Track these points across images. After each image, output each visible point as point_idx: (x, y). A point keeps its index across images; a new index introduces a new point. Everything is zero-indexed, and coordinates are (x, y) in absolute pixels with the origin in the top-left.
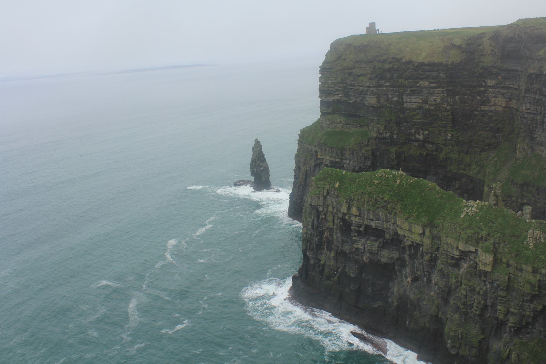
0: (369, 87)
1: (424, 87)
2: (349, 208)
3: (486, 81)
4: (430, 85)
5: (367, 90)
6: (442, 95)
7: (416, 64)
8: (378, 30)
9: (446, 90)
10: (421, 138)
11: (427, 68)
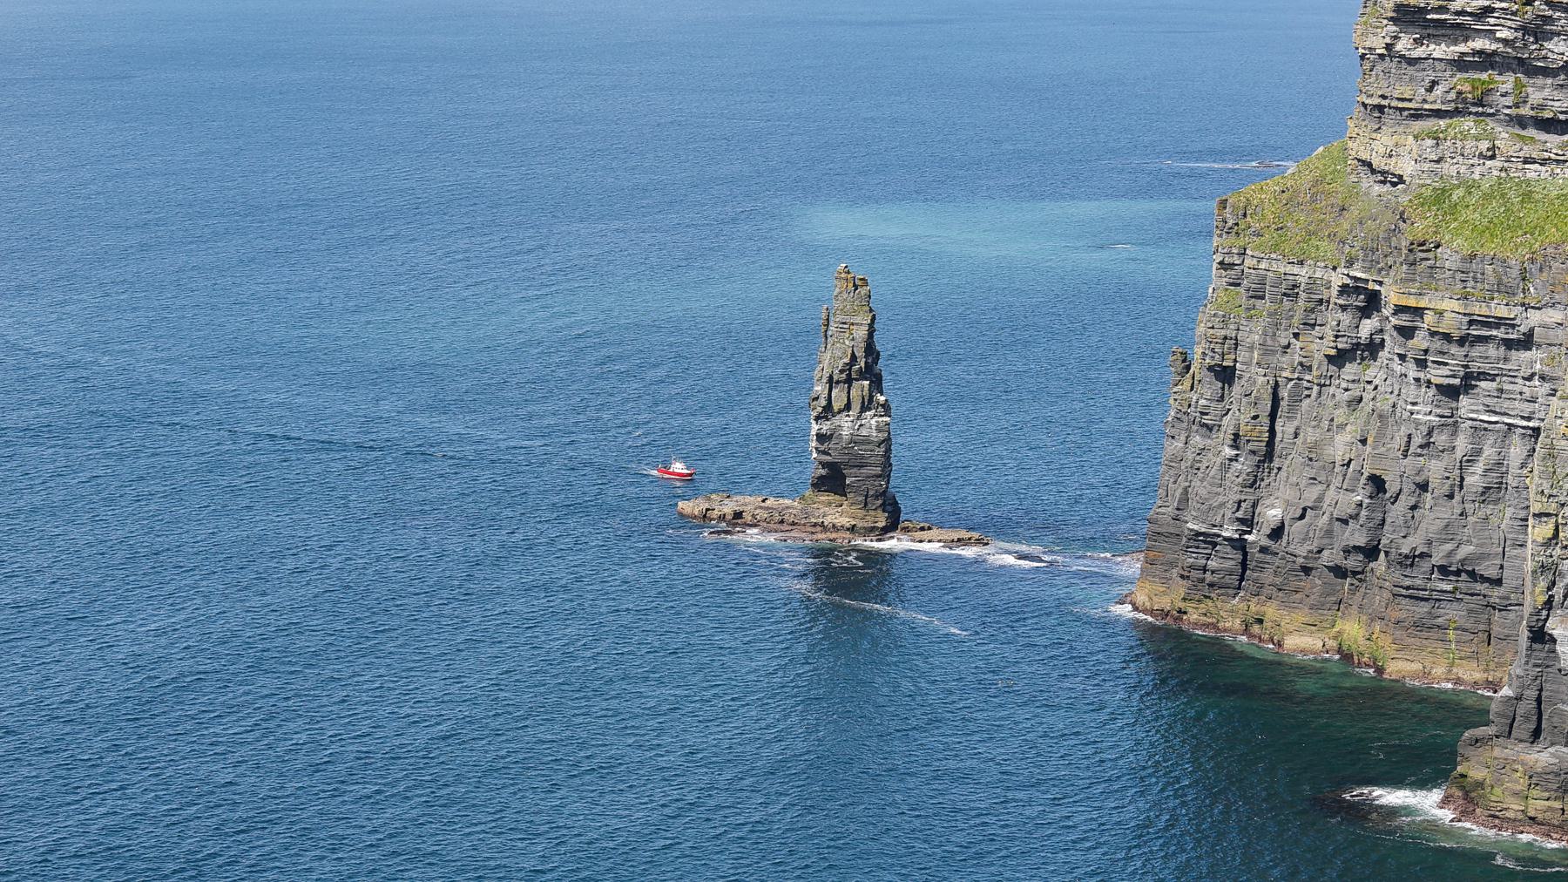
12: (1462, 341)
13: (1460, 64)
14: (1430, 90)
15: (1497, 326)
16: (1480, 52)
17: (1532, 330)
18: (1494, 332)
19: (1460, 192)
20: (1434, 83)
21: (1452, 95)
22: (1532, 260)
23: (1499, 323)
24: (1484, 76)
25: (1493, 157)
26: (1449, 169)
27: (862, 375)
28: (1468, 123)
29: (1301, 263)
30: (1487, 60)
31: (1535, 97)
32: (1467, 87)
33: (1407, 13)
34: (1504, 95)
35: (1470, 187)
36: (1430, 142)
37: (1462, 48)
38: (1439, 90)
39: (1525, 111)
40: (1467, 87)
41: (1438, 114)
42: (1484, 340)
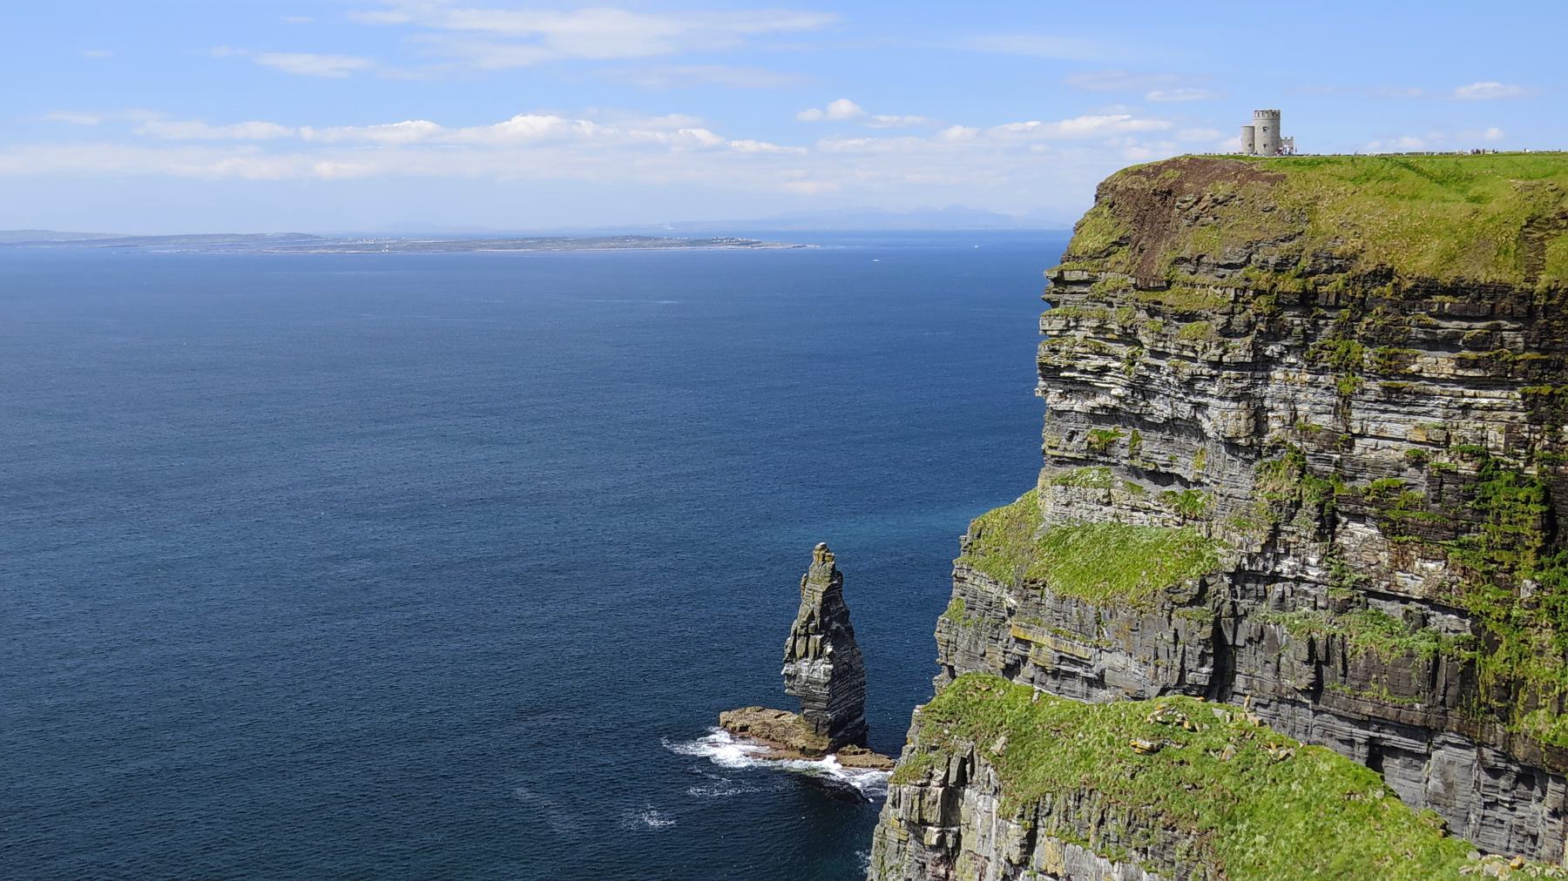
0: (1217, 365)
1: (1434, 381)
2: (1030, 842)
4: (1460, 372)
5: (1212, 378)
6: (1506, 415)
7: (1409, 284)
8: (1290, 141)
9: (1524, 396)
10: (1415, 586)
12: (1055, 674)
13: (1093, 416)
14: (1070, 439)
15: (1081, 664)
16: (1104, 407)
17: (1103, 671)
18: (1078, 670)
19: (1077, 535)
20: (1073, 433)
21: (1085, 446)
22: (1105, 606)
23: (1078, 662)
24: (1111, 429)
25: (1109, 504)
26: (1074, 512)
27: (817, 631)
28: (1093, 473)
29: (996, 583)
30: (1112, 415)
31: (1146, 448)
32: (1095, 439)
33: (1049, 371)
34: (1123, 446)
35: (1086, 529)
36: (1060, 488)
37: (1091, 403)
38: (1077, 439)
39: (1137, 462)
40: (1095, 439)
41: (1075, 461)
42: (1073, 675)
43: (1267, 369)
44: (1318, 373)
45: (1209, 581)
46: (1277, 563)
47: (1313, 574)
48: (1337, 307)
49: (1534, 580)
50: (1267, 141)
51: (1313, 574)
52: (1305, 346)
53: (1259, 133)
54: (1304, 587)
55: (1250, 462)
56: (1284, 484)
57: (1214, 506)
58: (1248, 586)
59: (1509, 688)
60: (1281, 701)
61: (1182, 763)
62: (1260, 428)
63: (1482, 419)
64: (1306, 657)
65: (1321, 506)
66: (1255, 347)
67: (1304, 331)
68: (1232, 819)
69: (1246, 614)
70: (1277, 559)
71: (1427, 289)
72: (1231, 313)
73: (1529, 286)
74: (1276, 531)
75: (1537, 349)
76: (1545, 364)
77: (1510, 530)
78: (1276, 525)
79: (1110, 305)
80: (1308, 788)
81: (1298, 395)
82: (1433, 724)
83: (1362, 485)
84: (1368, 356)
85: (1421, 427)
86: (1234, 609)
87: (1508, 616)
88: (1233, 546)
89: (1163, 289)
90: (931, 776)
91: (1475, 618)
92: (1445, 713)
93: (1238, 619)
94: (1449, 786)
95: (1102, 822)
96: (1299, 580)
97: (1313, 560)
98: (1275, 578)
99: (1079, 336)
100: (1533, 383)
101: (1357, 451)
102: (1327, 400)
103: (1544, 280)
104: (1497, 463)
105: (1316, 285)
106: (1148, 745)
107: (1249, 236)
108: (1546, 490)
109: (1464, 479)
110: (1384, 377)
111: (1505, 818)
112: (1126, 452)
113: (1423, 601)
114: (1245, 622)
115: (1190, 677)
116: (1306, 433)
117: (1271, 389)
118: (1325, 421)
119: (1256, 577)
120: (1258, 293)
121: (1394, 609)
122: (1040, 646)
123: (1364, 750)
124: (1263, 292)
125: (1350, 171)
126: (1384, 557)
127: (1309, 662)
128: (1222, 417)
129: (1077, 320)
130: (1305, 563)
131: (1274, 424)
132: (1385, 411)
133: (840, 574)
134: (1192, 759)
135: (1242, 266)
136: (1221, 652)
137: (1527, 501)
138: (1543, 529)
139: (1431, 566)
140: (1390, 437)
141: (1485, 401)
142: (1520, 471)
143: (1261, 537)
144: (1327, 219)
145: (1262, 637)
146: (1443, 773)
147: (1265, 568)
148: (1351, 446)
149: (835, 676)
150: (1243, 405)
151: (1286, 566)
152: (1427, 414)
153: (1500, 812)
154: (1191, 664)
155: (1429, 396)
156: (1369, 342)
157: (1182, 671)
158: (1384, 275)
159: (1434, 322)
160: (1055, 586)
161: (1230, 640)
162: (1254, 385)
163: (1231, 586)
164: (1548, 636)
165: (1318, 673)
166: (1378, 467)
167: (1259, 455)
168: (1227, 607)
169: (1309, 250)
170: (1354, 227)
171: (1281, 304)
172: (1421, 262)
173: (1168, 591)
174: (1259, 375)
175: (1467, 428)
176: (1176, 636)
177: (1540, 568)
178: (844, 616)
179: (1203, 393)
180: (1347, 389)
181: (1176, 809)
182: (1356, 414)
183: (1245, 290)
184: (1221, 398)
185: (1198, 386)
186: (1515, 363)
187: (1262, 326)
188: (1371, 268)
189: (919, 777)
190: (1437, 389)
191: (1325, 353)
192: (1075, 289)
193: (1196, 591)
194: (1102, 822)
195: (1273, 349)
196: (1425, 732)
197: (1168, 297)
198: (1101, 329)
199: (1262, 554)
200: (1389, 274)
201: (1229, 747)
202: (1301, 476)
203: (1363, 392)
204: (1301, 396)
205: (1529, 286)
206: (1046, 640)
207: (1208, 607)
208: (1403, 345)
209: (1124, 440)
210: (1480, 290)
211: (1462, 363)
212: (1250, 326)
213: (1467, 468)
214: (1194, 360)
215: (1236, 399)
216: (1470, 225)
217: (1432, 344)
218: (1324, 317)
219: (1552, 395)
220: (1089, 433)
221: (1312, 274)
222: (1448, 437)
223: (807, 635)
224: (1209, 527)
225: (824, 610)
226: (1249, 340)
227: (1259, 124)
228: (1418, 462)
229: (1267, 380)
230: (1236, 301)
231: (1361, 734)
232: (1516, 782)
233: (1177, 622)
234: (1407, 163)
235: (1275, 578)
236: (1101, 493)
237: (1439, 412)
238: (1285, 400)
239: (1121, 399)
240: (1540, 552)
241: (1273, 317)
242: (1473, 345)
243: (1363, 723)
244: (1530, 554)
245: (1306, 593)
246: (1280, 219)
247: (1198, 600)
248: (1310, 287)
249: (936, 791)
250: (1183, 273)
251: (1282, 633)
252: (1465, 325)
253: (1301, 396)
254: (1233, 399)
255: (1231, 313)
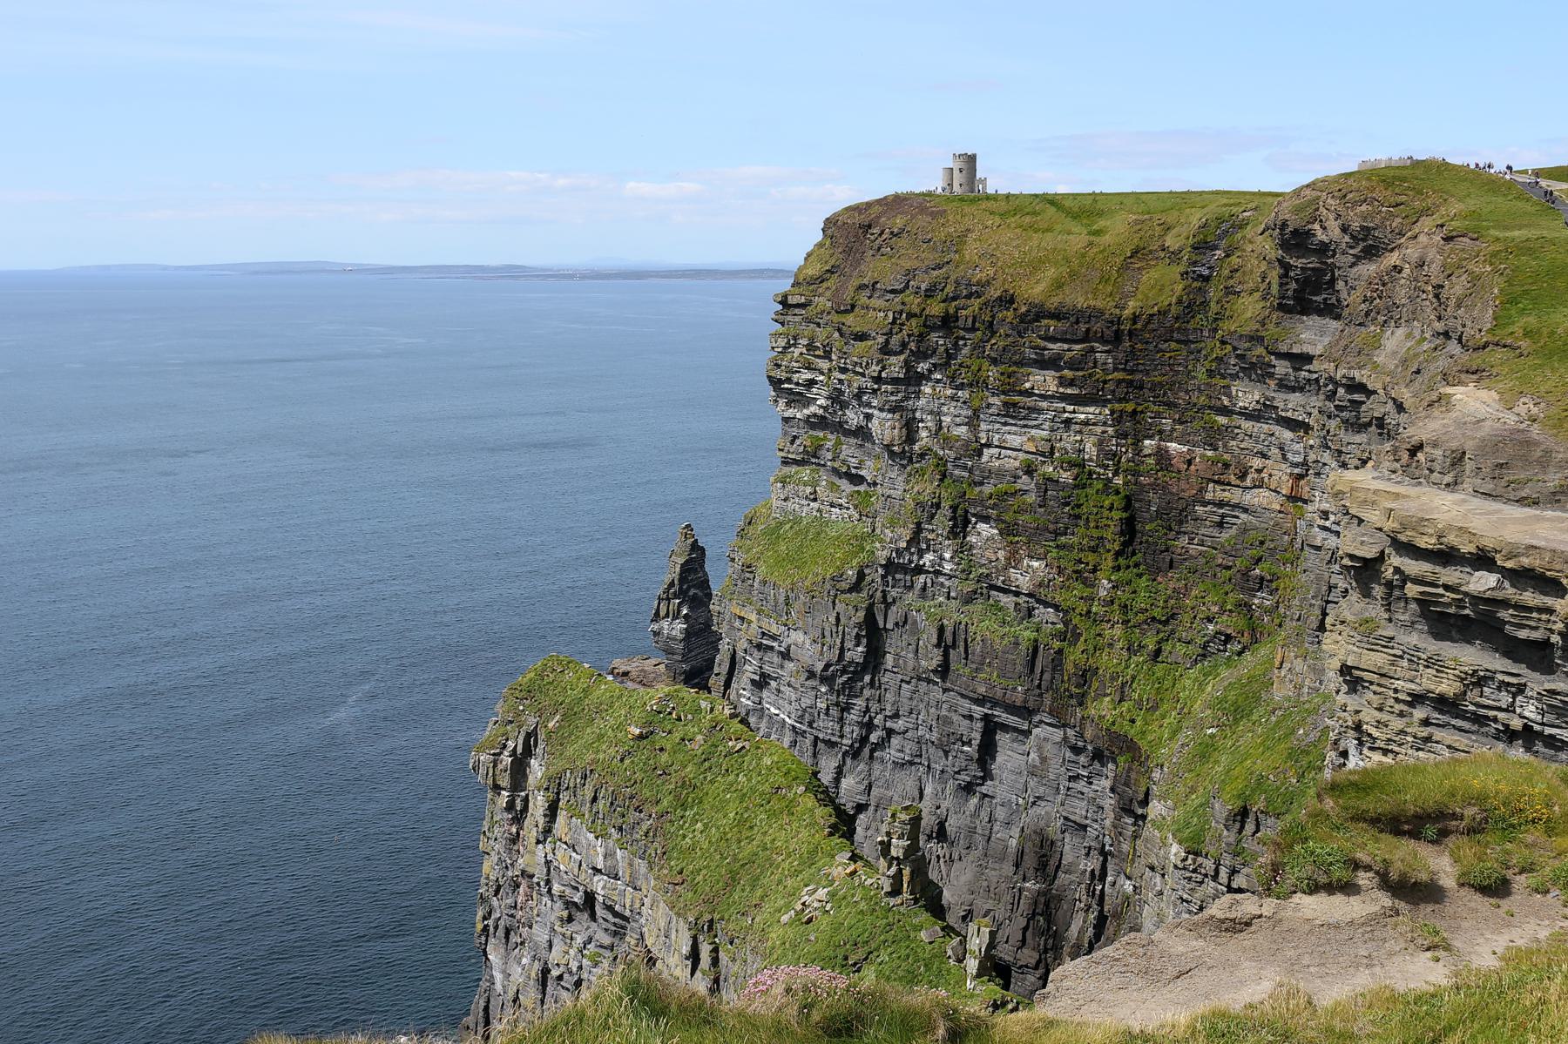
0: (878, 379)
1: (1043, 397)
3: (1234, 389)
5: (875, 391)
6: (1099, 429)
7: (1024, 309)
10: (1023, 582)
11: (1052, 326)
12: (759, 647)
14: (792, 442)
16: (815, 415)
18: (775, 644)
20: (795, 437)
23: (774, 638)
24: (821, 434)
25: (815, 500)
28: (805, 473)
31: (846, 451)
35: (797, 520)
38: (798, 442)
41: (796, 462)
43: (920, 385)
44: (957, 388)
45: (867, 571)
46: (921, 557)
47: (948, 567)
48: (973, 329)
49: (1110, 581)
50: (963, 181)
51: (948, 567)
52: (947, 364)
53: (956, 173)
54: (942, 579)
55: (905, 467)
56: (927, 488)
57: (878, 506)
58: (898, 576)
59: (1085, 676)
60: (919, 679)
61: (661, 750)
62: (911, 436)
63: (1080, 432)
64: (934, 640)
65: (954, 508)
66: (907, 365)
67: (947, 350)
68: (684, 806)
69: (894, 601)
70: (921, 554)
71: (1039, 313)
72: (890, 334)
73: (1118, 311)
74: (919, 529)
75: (1124, 370)
76: (1130, 383)
77: (1095, 533)
78: (918, 524)
79: (819, 325)
80: (749, 780)
81: (941, 407)
82: (1031, 705)
83: (988, 489)
84: (992, 373)
85: (1032, 439)
86: (884, 597)
87: (1089, 612)
88: (890, 539)
89: (846, 312)
90: (505, 746)
91: (1066, 612)
92: (1041, 695)
93: (888, 606)
94: (1043, 760)
95: (595, 799)
96: (938, 573)
97: (947, 556)
98: (920, 570)
99: (797, 352)
100: (1120, 401)
101: (985, 459)
102: (964, 413)
103: (1132, 305)
104: (1090, 473)
105: (957, 309)
106: (637, 731)
107: (908, 264)
108: (1128, 499)
109: (1065, 486)
110: (1004, 393)
111: (1085, 790)
112: (829, 456)
113: (1030, 595)
114: (894, 608)
115: (848, 655)
116: (947, 442)
117: (922, 402)
118: (962, 431)
119: (904, 569)
120: (911, 315)
121: (1007, 600)
122: (750, 622)
123: (979, 725)
124: (915, 315)
125: (1003, 206)
126: (1001, 554)
127: (938, 646)
128: (884, 427)
129: (795, 338)
130: (942, 558)
131: (924, 434)
132: (1005, 424)
133: (703, 550)
134: (668, 747)
135: (902, 291)
136: (872, 633)
137: (1111, 509)
138: (1122, 533)
139: (1036, 564)
140: (1011, 446)
141: (1083, 416)
142: (1110, 480)
143: (906, 534)
144: (971, 250)
145: (905, 622)
146: (1040, 748)
147: (911, 562)
148: (980, 454)
149: (688, 633)
150: (897, 416)
151: (928, 558)
152: (1037, 427)
153: (1080, 785)
154: (849, 644)
155: (1040, 411)
156: (994, 361)
157: (842, 649)
158: (1007, 301)
159: (1042, 343)
160: (762, 570)
161: (881, 625)
162: (907, 398)
163: (883, 577)
164: (1118, 631)
165: (946, 655)
166: (1000, 473)
167: (910, 461)
168: (879, 594)
169: (953, 277)
170: (989, 256)
171: (928, 327)
172: (1035, 290)
173: (833, 579)
174: (911, 389)
175: (1068, 441)
176: (838, 619)
177: (1117, 568)
178: (704, 584)
179: (869, 405)
180: (976, 403)
181: (647, 793)
182: (983, 426)
183: (901, 313)
184: (881, 410)
185: (865, 398)
186: (1105, 382)
187: (913, 346)
188: (998, 293)
189: (493, 747)
190: (1044, 404)
191: (963, 370)
192: (797, 311)
193: (854, 580)
194: (595, 799)
195: (923, 367)
196: (1026, 712)
197: (849, 319)
198: (810, 347)
199: (907, 549)
200: (1010, 300)
201: (699, 737)
202: (941, 480)
203: (989, 406)
204: (945, 409)
205: (1118, 311)
206: (753, 617)
207: (864, 594)
208: (1020, 364)
209: (829, 444)
210: (1079, 316)
211: (1062, 382)
212: (904, 345)
213: (1066, 477)
214: (863, 375)
215: (892, 411)
216: (1084, 256)
217: (1043, 364)
218: (963, 338)
219: (1134, 411)
220: (806, 438)
221: (954, 299)
222: (1052, 448)
223: (668, 599)
224: (873, 523)
225: (682, 579)
226: (902, 358)
227: (956, 166)
228: (1029, 470)
229: (918, 394)
230: (894, 322)
231: (978, 711)
232: (1093, 759)
233: (840, 607)
234: (1052, 201)
235: (920, 570)
236: (809, 490)
237: (1047, 425)
238: (931, 413)
239: (825, 408)
240: (1118, 554)
241: (921, 337)
242: (1072, 365)
243: (980, 701)
244: (1110, 556)
245: (942, 585)
246: (934, 249)
247: (856, 587)
248: (951, 311)
249: (507, 760)
250: (863, 299)
251: (920, 618)
252: (1066, 346)
253: (945, 409)
254: (889, 411)
255: (890, 334)
